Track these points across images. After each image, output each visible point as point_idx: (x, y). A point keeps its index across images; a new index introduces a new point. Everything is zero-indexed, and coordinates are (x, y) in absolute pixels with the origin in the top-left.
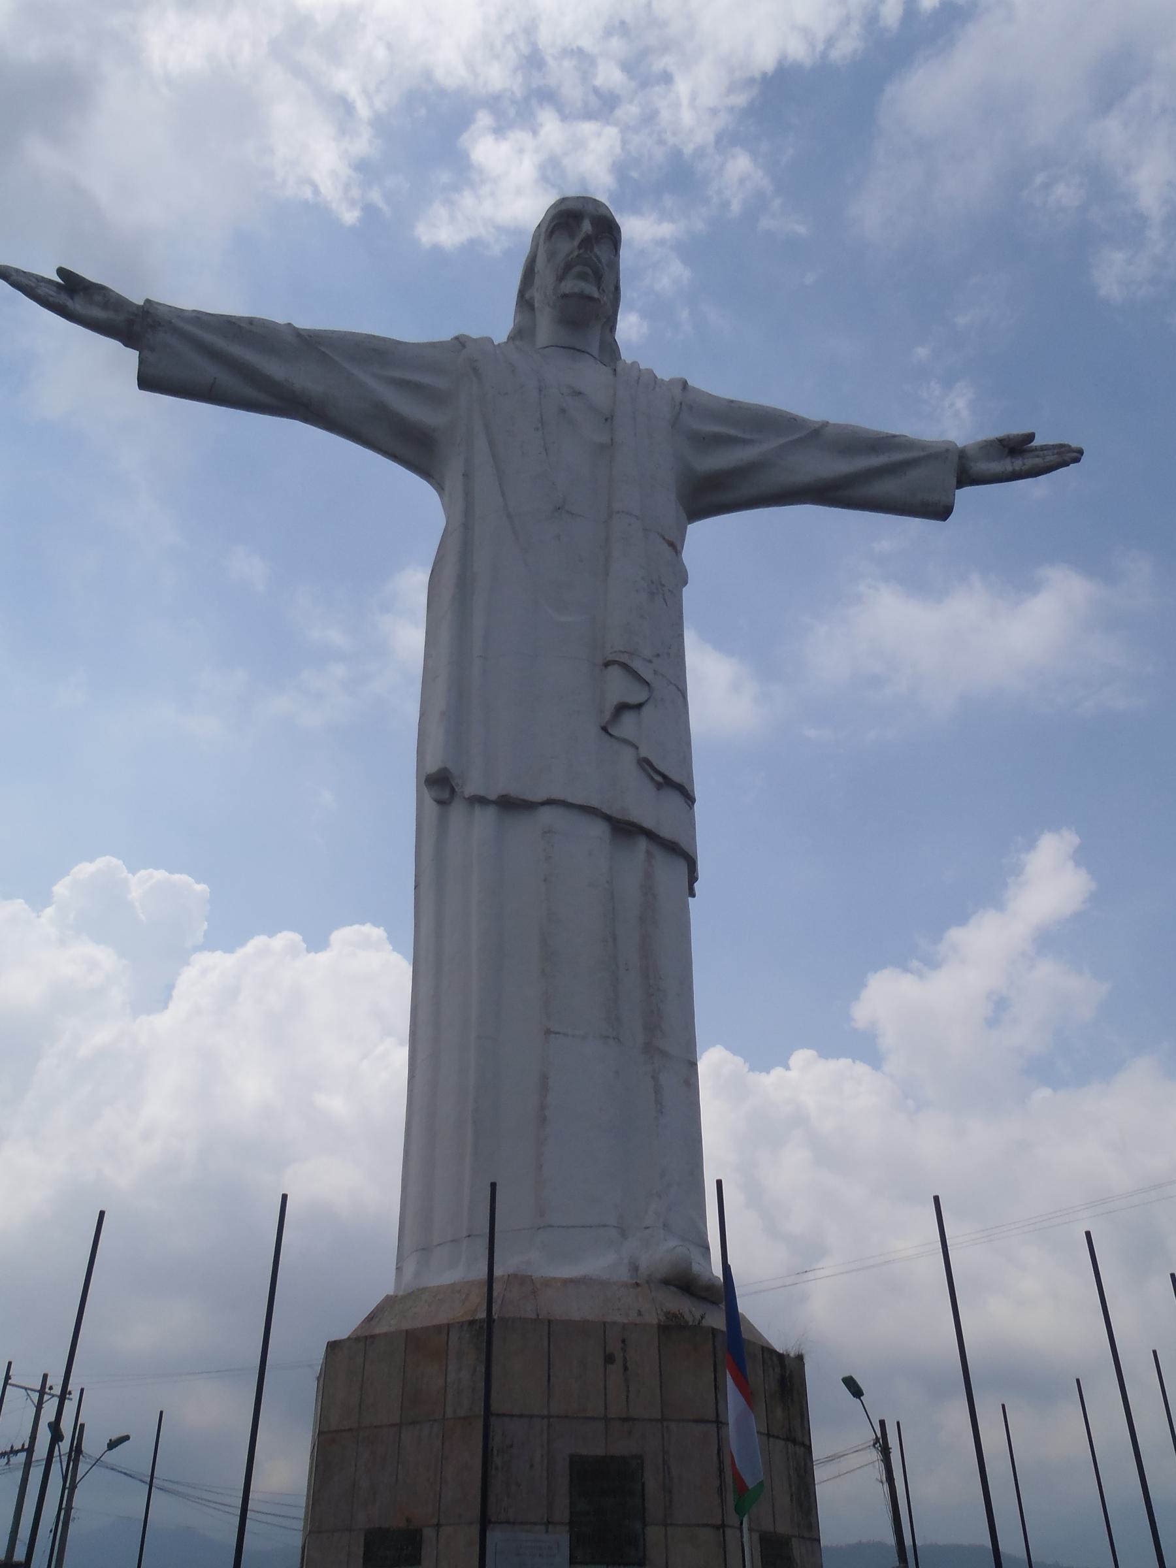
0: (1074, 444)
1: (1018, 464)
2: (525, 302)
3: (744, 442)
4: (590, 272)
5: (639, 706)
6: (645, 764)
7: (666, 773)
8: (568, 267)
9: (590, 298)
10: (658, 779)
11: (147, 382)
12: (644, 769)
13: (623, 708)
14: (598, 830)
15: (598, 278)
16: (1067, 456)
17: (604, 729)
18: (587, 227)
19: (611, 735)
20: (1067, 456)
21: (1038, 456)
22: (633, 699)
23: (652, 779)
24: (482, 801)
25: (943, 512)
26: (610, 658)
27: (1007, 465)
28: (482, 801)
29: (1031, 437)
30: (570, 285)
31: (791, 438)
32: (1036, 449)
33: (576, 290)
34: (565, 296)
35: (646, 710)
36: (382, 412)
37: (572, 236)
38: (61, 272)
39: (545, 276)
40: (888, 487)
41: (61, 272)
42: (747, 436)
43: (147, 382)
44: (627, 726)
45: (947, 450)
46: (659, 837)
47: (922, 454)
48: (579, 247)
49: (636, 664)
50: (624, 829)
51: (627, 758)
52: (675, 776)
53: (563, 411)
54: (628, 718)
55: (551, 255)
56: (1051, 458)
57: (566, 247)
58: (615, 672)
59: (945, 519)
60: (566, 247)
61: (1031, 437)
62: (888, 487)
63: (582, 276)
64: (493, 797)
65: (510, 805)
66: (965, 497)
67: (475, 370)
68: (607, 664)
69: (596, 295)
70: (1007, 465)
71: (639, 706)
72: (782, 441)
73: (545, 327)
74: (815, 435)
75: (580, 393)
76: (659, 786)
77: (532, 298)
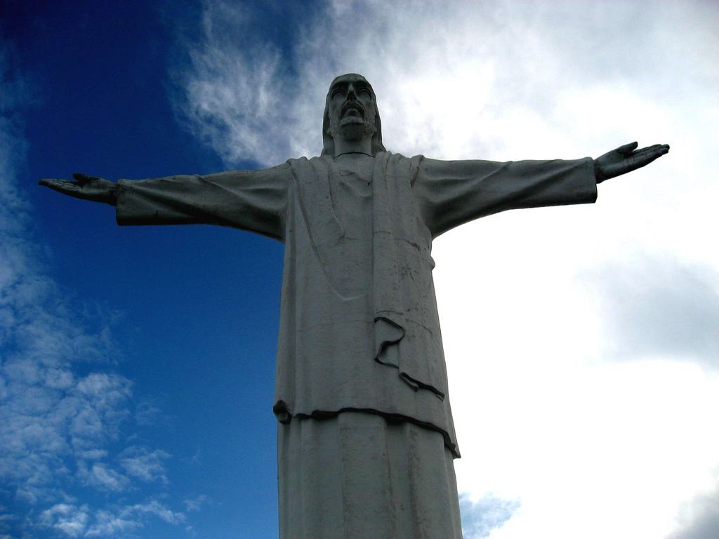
1: (631, 161)
2: (327, 136)
3: (463, 182)
4: (356, 110)
5: (397, 342)
6: (404, 377)
7: (419, 380)
8: (344, 111)
9: (358, 124)
10: (415, 385)
12: (405, 382)
13: (386, 346)
14: (378, 422)
15: (362, 113)
16: (660, 150)
17: (377, 360)
18: (351, 88)
19: (381, 363)
20: (660, 150)
21: (643, 154)
22: (392, 339)
23: (410, 386)
24: (302, 417)
25: (591, 198)
26: (376, 316)
27: (625, 163)
29: (635, 144)
30: (346, 120)
31: (491, 174)
32: (641, 151)
33: (349, 121)
34: (344, 126)
35: (403, 344)
36: (249, 210)
37: (344, 95)
39: (334, 119)
40: (555, 190)
42: (464, 178)
44: (391, 355)
45: (587, 162)
46: (418, 421)
47: (572, 167)
48: (348, 99)
49: (391, 317)
50: (395, 421)
51: (393, 374)
52: (425, 381)
53: (342, 184)
54: (391, 351)
55: (334, 107)
56: (650, 154)
57: (341, 101)
58: (380, 323)
59: (594, 202)
60: (341, 101)
61: (635, 144)
62: (555, 190)
63: (353, 114)
64: (310, 414)
65: (322, 417)
66: (602, 188)
67: (294, 174)
68: (376, 320)
69: (360, 120)
70: (625, 163)
71: (397, 342)
72: (485, 177)
73: (339, 147)
74: (506, 170)
75: (352, 173)
76: (415, 389)
77: (330, 133)
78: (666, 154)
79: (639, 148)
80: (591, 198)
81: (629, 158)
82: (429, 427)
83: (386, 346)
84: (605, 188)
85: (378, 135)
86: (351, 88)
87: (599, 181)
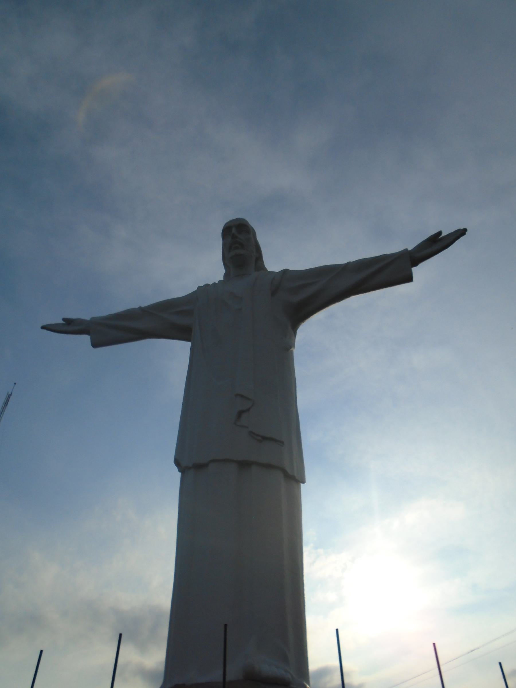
0: (462, 228)
5: (248, 410)
11: (95, 345)
13: (240, 414)
16: (461, 233)
18: (234, 231)
25: (409, 279)
29: (440, 233)
38: (64, 319)
41: (64, 319)
43: (95, 345)
50: (244, 465)
71: (248, 410)
78: (465, 236)
79: (444, 234)
80: (409, 279)
81: (436, 244)
82: (269, 466)
83: (240, 414)
86: (234, 231)
87: (415, 263)
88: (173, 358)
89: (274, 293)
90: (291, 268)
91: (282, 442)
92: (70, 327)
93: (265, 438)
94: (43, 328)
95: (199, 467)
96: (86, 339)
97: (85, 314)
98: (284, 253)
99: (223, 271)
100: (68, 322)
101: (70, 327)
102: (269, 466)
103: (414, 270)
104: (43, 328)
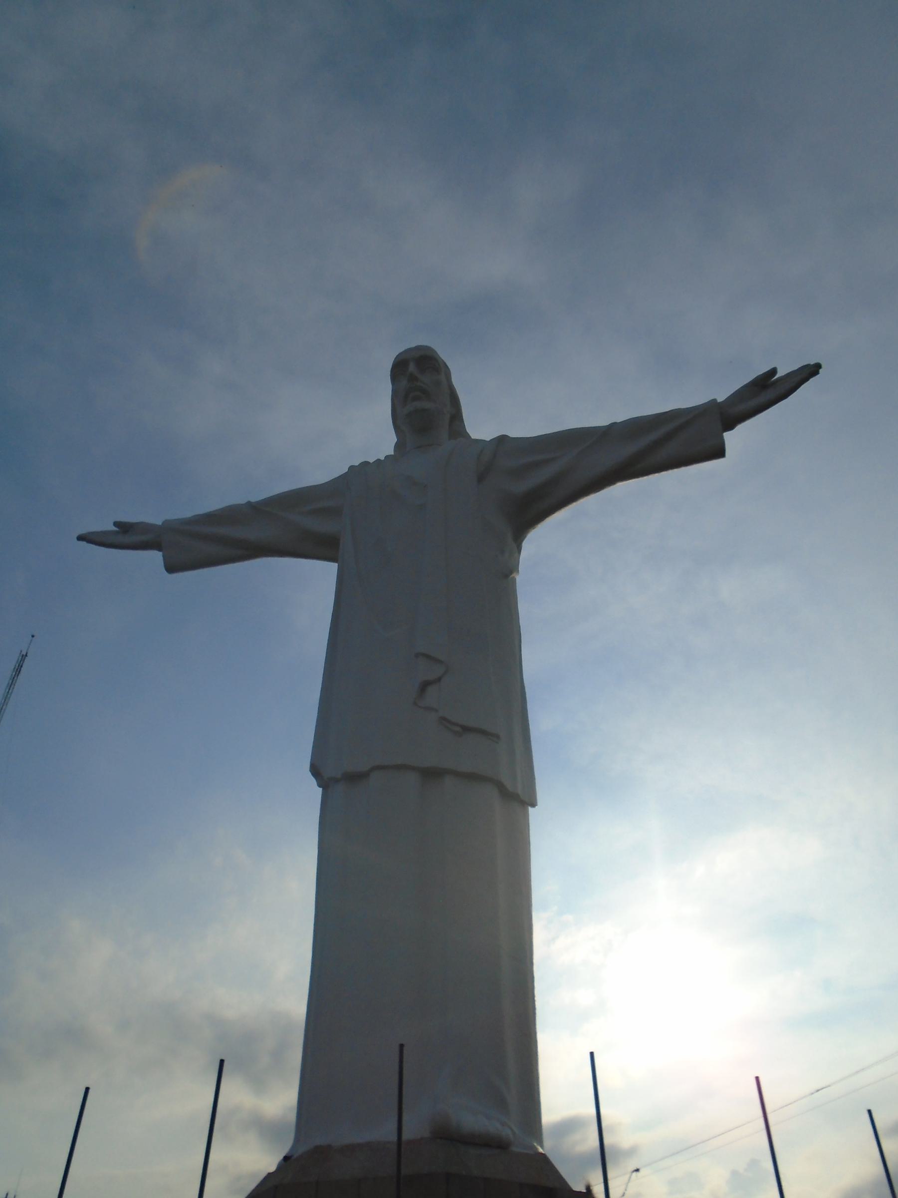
5: (439, 680)
6: (444, 721)
10: (458, 729)
13: (425, 686)
16: (812, 371)
18: (412, 368)
24: (336, 781)
25: (719, 452)
28: (336, 781)
29: (773, 371)
38: (116, 524)
41: (116, 524)
43: (171, 568)
50: (431, 775)
69: (427, 405)
71: (439, 680)
80: (719, 452)
81: (766, 391)
82: (473, 777)
83: (425, 686)
84: (734, 439)
85: (457, 416)
86: (412, 368)
87: (730, 425)
88: (308, 591)
89: (481, 478)
90: (514, 433)
91: (498, 737)
92: (127, 536)
93: (466, 729)
94: (80, 538)
95: (354, 778)
96: (155, 557)
97: (152, 515)
98: (499, 407)
99: (391, 439)
100: (124, 528)
101: (127, 536)
102: (473, 777)
103: (727, 435)
104: (80, 538)
